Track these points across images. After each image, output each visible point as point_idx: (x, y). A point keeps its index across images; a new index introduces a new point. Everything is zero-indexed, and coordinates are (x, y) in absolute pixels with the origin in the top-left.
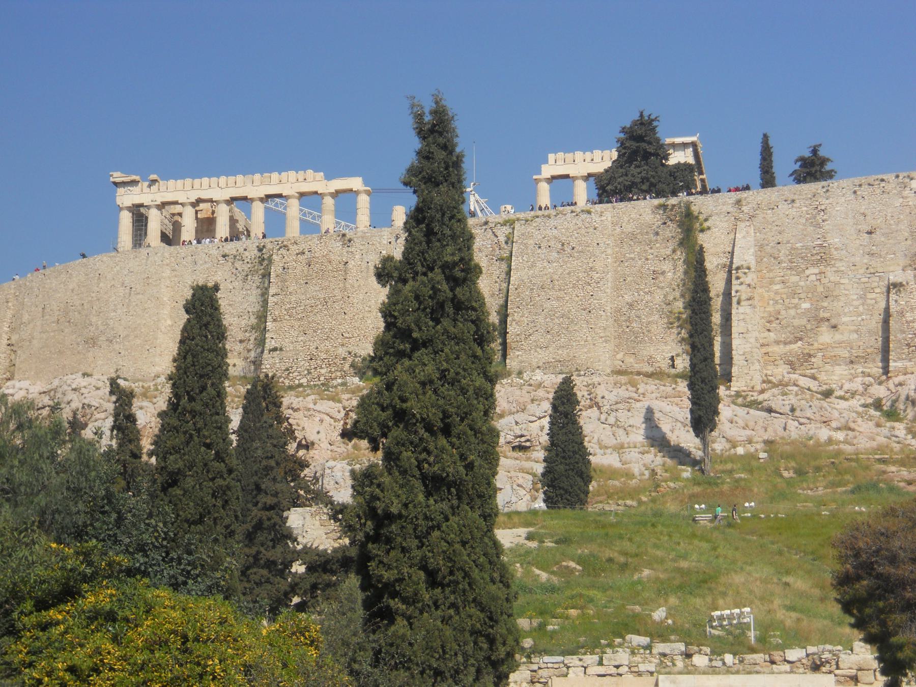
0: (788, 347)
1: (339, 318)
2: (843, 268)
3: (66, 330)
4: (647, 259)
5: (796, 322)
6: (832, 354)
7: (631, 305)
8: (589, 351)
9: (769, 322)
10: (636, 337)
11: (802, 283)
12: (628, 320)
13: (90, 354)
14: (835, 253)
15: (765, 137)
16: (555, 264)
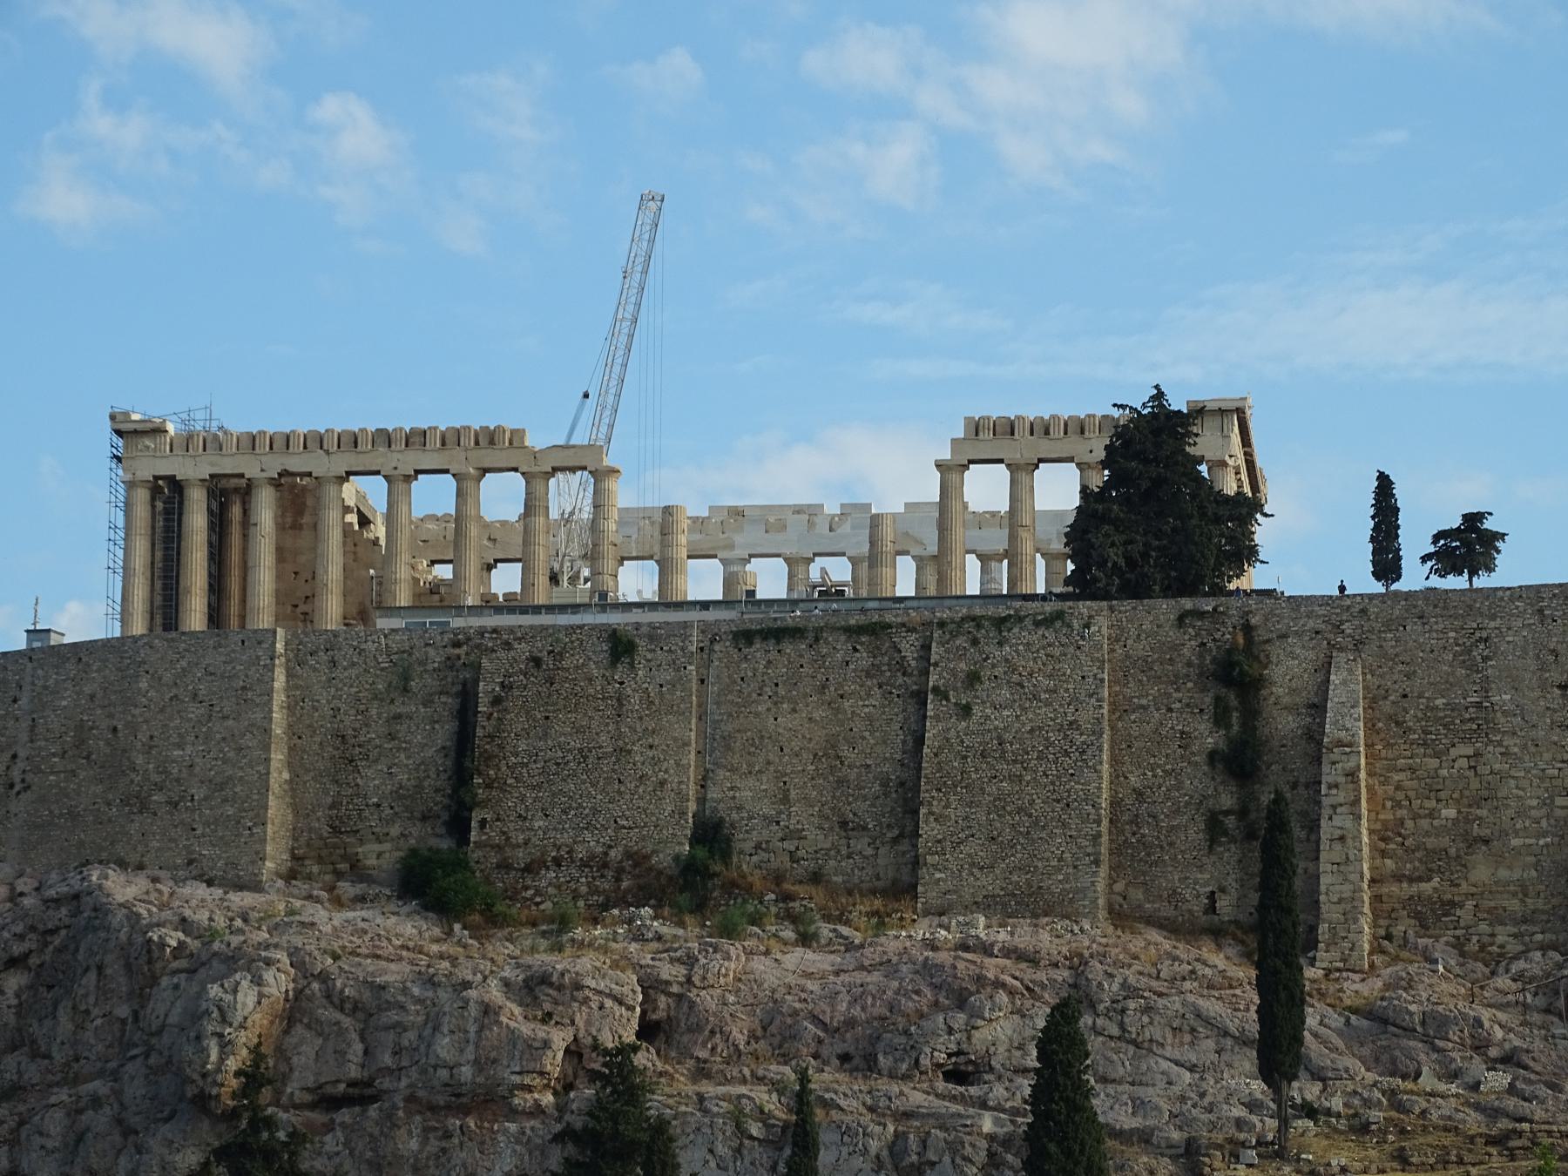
0: (1414, 889)
1: (609, 788)
2: (1516, 750)
3: (82, 774)
4: (1170, 710)
5: (1431, 842)
6: (1492, 904)
7: (1139, 794)
8: (1066, 880)
9: (1383, 839)
10: (1148, 855)
11: (1444, 772)
12: (1135, 820)
13: (134, 828)
14: (1503, 720)
15: (1384, 486)
16: (1006, 713)
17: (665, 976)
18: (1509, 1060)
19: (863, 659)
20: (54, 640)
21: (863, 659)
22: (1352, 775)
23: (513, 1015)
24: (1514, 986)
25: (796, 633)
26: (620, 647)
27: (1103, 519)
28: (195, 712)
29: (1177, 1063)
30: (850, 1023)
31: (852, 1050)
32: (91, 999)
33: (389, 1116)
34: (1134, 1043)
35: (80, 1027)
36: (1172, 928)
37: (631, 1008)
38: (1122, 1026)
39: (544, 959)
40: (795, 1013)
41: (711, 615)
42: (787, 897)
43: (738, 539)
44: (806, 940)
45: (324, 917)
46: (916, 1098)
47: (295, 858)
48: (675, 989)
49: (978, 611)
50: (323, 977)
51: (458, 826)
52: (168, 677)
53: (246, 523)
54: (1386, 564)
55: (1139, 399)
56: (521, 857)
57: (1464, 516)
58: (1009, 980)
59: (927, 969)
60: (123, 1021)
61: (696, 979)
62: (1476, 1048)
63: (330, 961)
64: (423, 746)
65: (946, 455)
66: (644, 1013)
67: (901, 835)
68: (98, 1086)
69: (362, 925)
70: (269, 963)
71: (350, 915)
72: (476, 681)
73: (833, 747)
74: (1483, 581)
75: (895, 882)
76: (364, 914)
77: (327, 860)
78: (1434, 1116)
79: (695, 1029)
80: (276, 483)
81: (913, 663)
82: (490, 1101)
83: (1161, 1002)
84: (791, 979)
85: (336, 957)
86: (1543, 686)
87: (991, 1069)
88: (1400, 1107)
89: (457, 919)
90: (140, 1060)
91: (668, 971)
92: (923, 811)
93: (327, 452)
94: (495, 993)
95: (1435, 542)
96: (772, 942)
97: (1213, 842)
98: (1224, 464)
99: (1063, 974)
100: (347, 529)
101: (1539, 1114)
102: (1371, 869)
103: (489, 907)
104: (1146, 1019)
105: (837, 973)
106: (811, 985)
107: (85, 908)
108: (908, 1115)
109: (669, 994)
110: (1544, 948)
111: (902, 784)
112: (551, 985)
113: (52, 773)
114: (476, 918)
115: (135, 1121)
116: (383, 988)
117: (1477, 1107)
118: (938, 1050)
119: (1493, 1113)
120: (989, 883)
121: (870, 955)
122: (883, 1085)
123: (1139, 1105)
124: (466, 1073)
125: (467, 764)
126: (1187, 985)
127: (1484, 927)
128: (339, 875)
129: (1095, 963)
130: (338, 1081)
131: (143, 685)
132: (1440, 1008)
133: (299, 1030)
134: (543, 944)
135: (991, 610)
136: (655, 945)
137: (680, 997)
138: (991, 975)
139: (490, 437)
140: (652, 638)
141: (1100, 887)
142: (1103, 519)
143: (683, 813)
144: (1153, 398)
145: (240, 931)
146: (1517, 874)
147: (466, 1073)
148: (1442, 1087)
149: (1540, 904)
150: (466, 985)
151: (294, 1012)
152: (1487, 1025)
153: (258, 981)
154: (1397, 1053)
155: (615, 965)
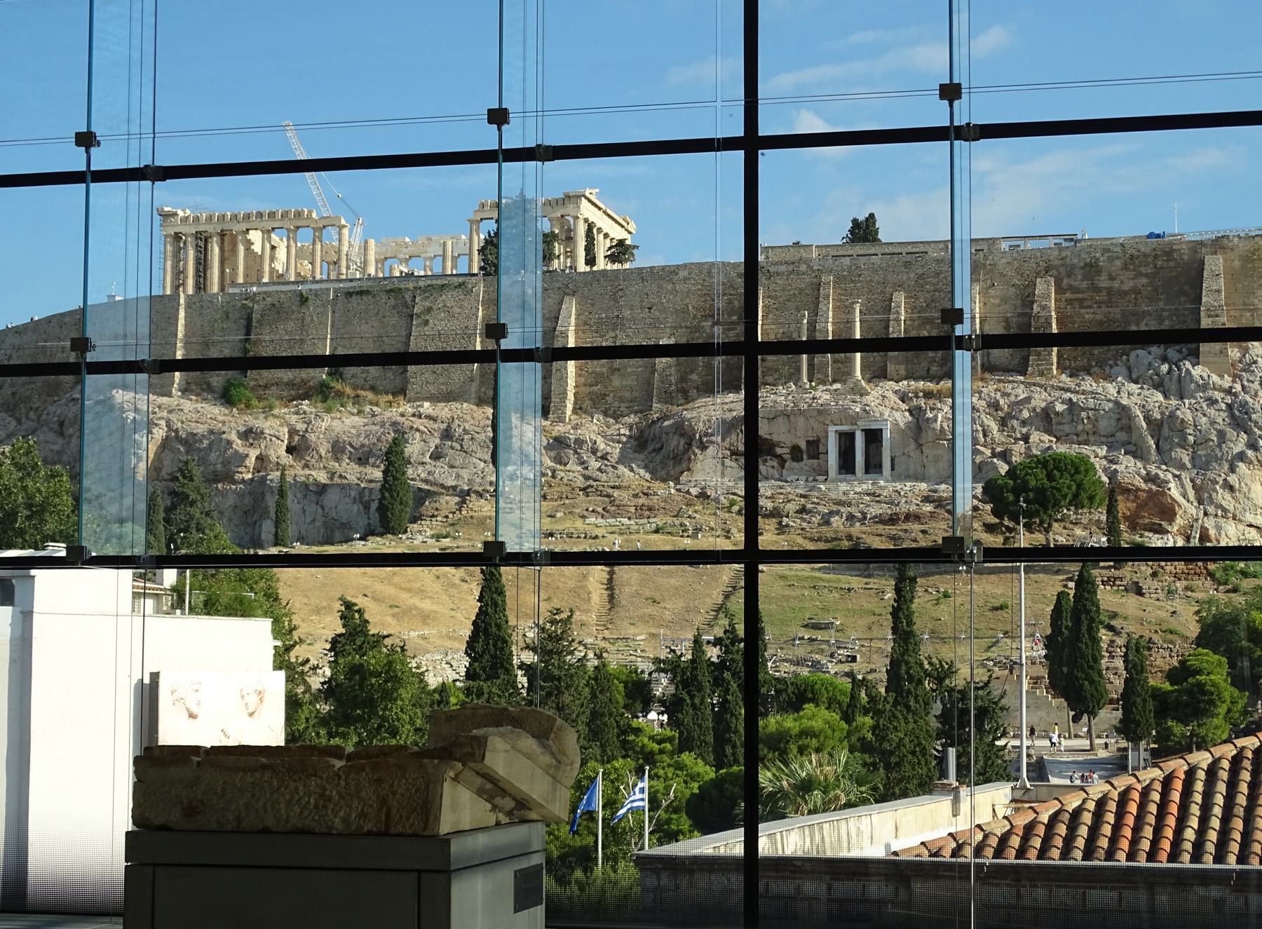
19: (392, 302)
20: (117, 298)
21: (392, 302)
23: (238, 445)
25: (368, 292)
26: (303, 300)
30: (363, 446)
41: (336, 285)
42: (358, 396)
44: (360, 412)
47: (188, 383)
49: (434, 282)
50: (177, 431)
58: (422, 428)
59: (394, 424)
65: (471, 217)
74: (627, 266)
79: (308, 448)
80: (222, 235)
82: (229, 477)
84: (346, 429)
86: (642, 308)
88: (553, 477)
91: (301, 427)
94: (233, 437)
99: (445, 425)
108: (371, 481)
110: (636, 413)
114: (243, 406)
117: (584, 476)
119: (587, 478)
123: (458, 476)
124: (219, 467)
127: (616, 404)
128: (203, 390)
135: (439, 282)
137: (303, 436)
139: (299, 214)
140: (316, 295)
141: (473, 389)
147: (219, 467)
149: (637, 394)
151: (165, 444)
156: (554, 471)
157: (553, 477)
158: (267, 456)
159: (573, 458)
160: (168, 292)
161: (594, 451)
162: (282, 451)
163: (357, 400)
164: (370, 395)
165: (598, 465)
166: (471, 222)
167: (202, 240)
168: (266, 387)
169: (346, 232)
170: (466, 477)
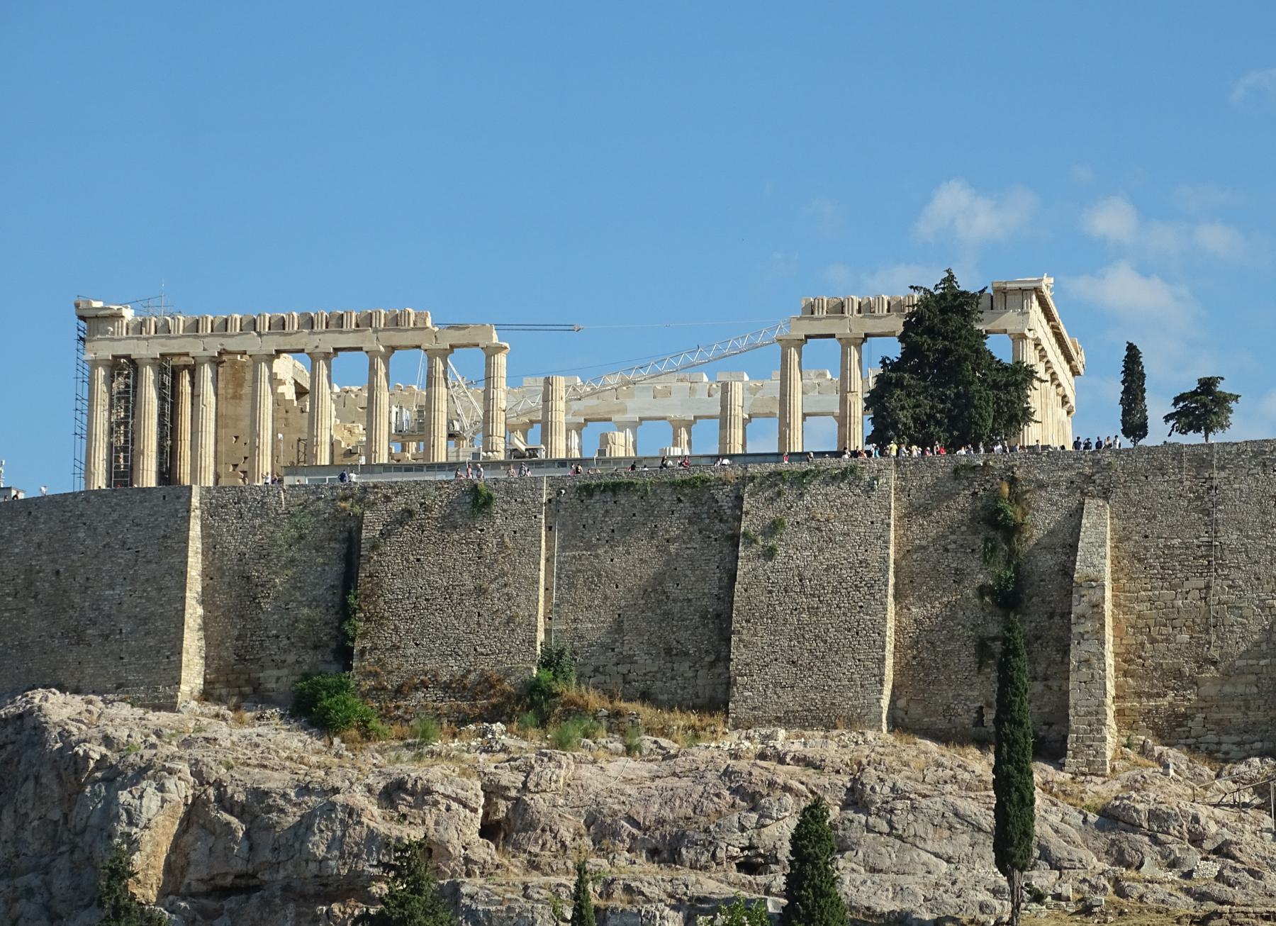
3: (31, 611)
6: (1219, 716)
9: (1125, 661)
10: (927, 675)
14: (1230, 556)
15: (1132, 356)
17: (504, 783)
18: (1222, 851)
21: (687, 508)
22: (1097, 606)
24: (1234, 787)
27: (899, 384)
28: (124, 557)
29: (937, 855)
30: (661, 822)
31: (660, 846)
32: (29, 805)
33: (267, 903)
34: (900, 838)
35: (21, 828)
36: (942, 737)
37: (474, 810)
38: (890, 823)
39: (409, 769)
40: (615, 813)
42: (617, 714)
43: (630, 404)
44: (629, 750)
45: (225, 732)
46: (709, 885)
48: (513, 793)
50: (218, 784)
51: (344, 656)
52: (101, 528)
53: (195, 396)
54: (1135, 426)
55: (932, 280)
56: (391, 683)
57: (1200, 380)
58: (795, 784)
60: (56, 823)
61: (531, 785)
62: (1192, 842)
63: (223, 770)
64: (315, 585)
66: (486, 815)
67: (717, 659)
68: (34, 880)
69: (256, 739)
70: (171, 772)
71: (247, 731)
72: (360, 529)
73: (660, 584)
74: (1216, 438)
75: (712, 699)
76: (260, 730)
77: (235, 685)
78: (1150, 900)
79: (531, 826)
80: (216, 362)
81: (729, 512)
83: (924, 802)
84: (613, 784)
85: (229, 767)
87: (777, 862)
88: (1121, 892)
89: (336, 734)
90: (66, 856)
91: (509, 778)
92: (734, 638)
93: (260, 335)
94: (359, 798)
95: (1175, 404)
96: (601, 753)
97: (981, 664)
98: (1024, 337)
100: (279, 400)
101: (1240, 897)
102: (1117, 687)
103: (365, 723)
104: (911, 817)
105: (653, 780)
106: (629, 789)
107: (30, 727)
109: (507, 798)
110: (1262, 755)
111: (718, 616)
112: (406, 791)
113: (6, 610)
114: (354, 733)
115: (60, 908)
116: (267, 794)
117: (1188, 892)
118: (733, 844)
119: (1202, 897)
120: (789, 700)
121: (681, 763)
122: (686, 875)
123: (899, 891)
125: (351, 599)
126: (948, 787)
129: (870, 770)
130: (227, 874)
131: (81, 535)
132: (1163, 807)
133: (194, 830)
134: (407, 755)
136: (502, 756)
137: (517, 800)
138: (780, 781)
139: (395, 322)
140: (509, 491)
142: (899, 384)
143: (532, 642)
144: (944, 281)
145: (153, 746)
146: (1241, 689)
148: (1160, 874)
149: (1260, 716)
150: (336, 791)
151: (193, 815)
152: (1203, 821)
153: (161, 788)
154: (1125, 845)
155: (463, 773)
156: (1116, 881)
157: (1121, 892)
158: (443, 845)
159: (1151, 855)
160: (100, 482)
161: (1197, 839)
162: (472, 833)
163: (616, 722)
164: (646, 713)
165: (1212, 868)
166: (786, 344)
167: (172, 372)
168: (399, 692)
169: (501, 360)
170: (920, 892)
